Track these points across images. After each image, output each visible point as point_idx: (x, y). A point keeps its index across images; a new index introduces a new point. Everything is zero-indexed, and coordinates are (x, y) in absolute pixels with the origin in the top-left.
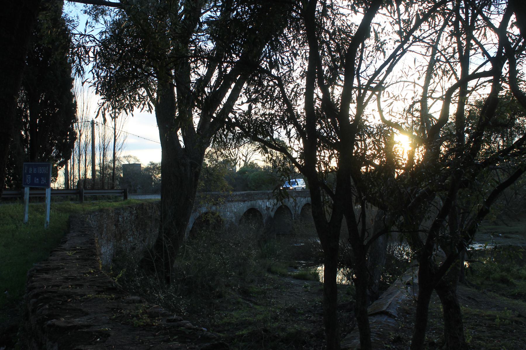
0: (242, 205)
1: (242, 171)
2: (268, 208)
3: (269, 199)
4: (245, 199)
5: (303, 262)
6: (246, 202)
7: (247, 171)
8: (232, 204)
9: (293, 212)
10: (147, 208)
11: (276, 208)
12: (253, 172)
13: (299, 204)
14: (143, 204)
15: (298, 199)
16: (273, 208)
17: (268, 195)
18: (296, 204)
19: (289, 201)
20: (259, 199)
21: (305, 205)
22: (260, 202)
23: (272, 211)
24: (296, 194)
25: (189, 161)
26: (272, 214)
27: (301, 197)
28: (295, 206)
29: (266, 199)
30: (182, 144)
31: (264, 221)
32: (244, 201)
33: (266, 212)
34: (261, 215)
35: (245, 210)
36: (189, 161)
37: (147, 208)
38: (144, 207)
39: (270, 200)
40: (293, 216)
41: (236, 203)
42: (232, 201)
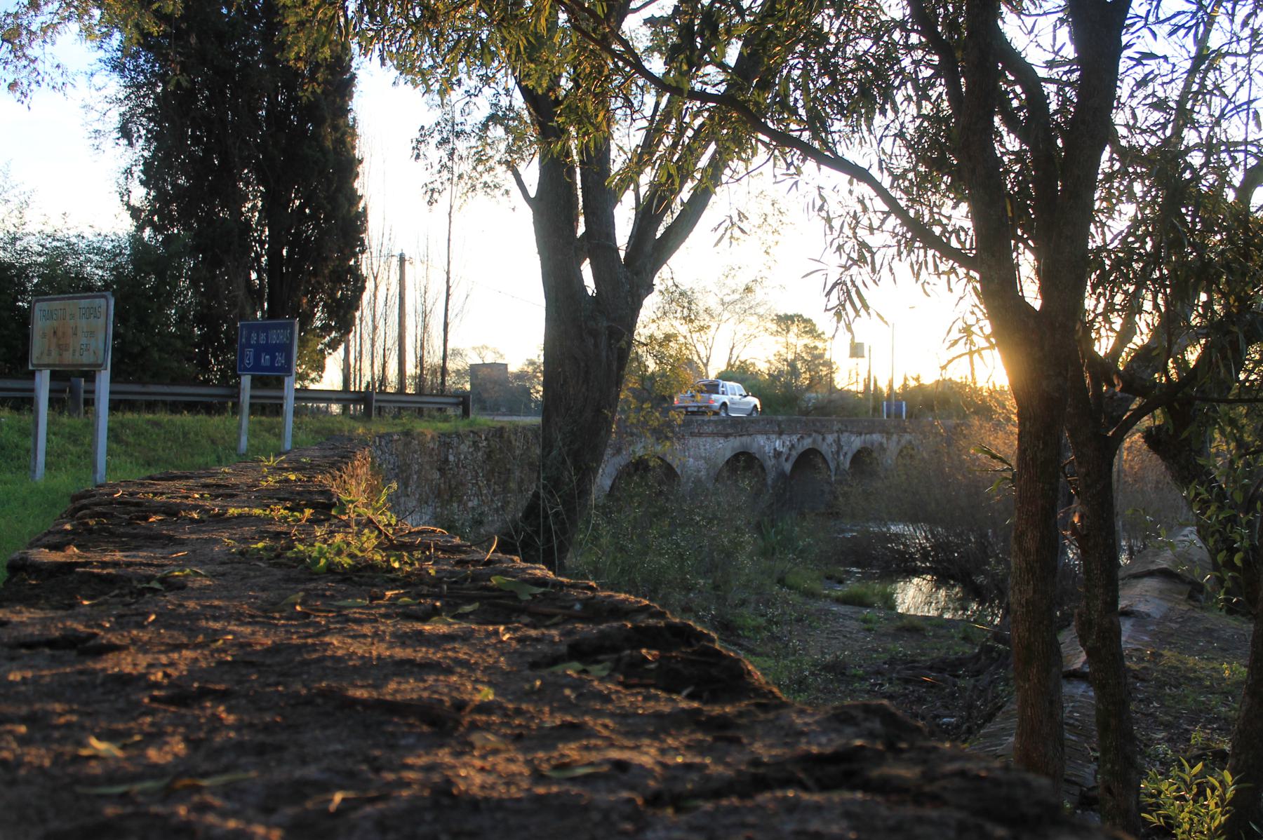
2: (778, 454)
3: (781, 433)
4: (729, 431)
5: (855, 569)
6: (731, 439)
8: (701, 441)
9: (832, 466)
11: (795, 454)
13: (845, 449)
16: (789, 455)
17: (779, 426)
18: (840, 447)
19: (824, 439)
22: (761, 440)
23: (787, 460)
24: (840, 425)
26: (788, 467)
27: (852, 432)
28: (838, 453)
29: (774, 432)
31: (769, 482)
32: (727, 436)
33: (773, 461)
34: (763, 469)
35: (729, 454)
37: (513, 437)
38: (506, 435)
39: (784, 437)
41: (709, 440)
42: (700, 435)
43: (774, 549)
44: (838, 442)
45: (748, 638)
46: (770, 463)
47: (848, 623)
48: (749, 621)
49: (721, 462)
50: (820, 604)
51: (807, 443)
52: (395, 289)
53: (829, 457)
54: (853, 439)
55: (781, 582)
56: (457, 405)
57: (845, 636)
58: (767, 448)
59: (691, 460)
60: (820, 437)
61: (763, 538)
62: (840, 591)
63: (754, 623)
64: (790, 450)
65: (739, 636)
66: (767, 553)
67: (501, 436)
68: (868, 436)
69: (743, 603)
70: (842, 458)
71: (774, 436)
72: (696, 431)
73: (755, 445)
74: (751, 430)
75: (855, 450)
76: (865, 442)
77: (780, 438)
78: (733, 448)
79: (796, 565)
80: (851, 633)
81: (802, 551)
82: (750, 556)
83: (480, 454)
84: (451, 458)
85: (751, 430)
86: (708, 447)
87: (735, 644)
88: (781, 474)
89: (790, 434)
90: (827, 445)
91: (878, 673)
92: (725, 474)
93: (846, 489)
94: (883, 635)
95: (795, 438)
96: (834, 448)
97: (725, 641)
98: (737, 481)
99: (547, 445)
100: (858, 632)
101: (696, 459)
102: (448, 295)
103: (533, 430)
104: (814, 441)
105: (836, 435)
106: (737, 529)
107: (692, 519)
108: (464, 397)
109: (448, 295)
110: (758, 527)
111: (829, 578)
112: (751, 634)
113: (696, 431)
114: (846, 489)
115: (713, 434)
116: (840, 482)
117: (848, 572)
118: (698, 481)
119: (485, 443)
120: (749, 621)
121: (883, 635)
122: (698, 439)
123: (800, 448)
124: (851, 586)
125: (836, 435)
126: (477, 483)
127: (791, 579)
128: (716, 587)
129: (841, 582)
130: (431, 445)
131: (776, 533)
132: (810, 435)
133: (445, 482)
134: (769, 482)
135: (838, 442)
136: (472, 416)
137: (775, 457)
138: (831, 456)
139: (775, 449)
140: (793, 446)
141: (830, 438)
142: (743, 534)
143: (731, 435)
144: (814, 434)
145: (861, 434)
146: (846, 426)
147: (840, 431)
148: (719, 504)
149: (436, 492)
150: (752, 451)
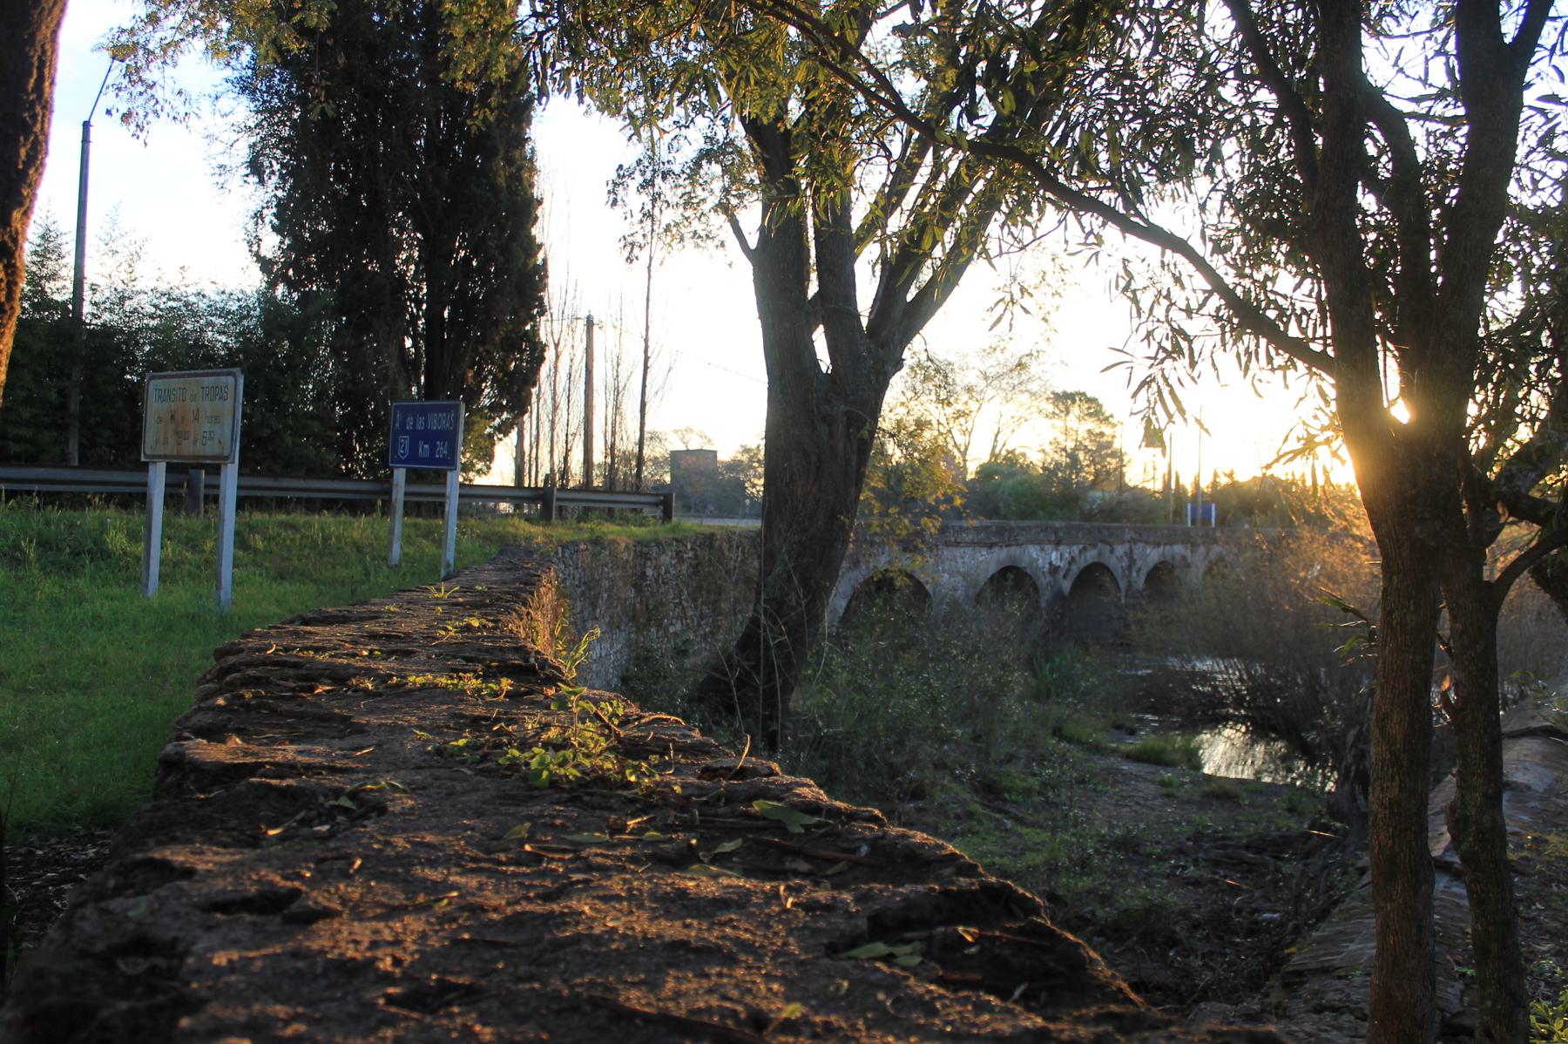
0: (983, 555)
2: (1054, 570)
3: (1058, 543)
4: (994, 539)
5: (1149, 717)
6: (996, 549)
8: (958, 552)
9: (1123, 585)
10: (725, 546)
11: (1075, 569)
13: (1139, 563)
16: (1068, 570)
18: (1132, 561)
19: (1112, 551)
22: (1033, 551)
23: (1065, 576)
24: (1132, 534)
26: (1066, 585)
27: (1147, 542)
28: (1130, 568)
29: (1050, 542)
31: (1043, 604)
32: (990, 546)
33: (1049, 578)
34: (1036, 588)
35: (993, 569)
37: (725, 546)
38: (717, 544)
39: (1061, 548)
41: (969, 550)
42: (957, 544)
43: (1049, 690)
44: (1130, 554)
46: (1044, 581)
47: (1141, 786)
48: (1018, 781)
49: (983, 579)
51: (1091, 556)
53: (1118, 573)
54: (1148, 551)
55: (1058, 732)
56: (656, 505)
57: (1137, 803)
58: (1040, 561)
59: (946, 575)
60: (1108, 548)
61: (1035, 676)
62: (1132, 744)
63: (1024, 784)
64: (1070, 563)
65: (1005, 800)
66: (1040, 695)
67: (711, 546)
68: (1168, 548)
69: (1010, 758)
70: (1134, 574)
73: (1026, 558)
74: (1021, 539)
75: (1151, 565)
76: (1163, 554)
77: (1057, 550)
79: (1077, 711)
80: (1146, 799)
81: (1084, 694)
82: (1020, 700)
83: (684, 567)
84: (649, 572)
85: (1021, 539)
86: (966, 560)
87: (1000, 811)
89: (1070, 544)
90: (1116, 557)
91: (1180, 852)
92: (988, 594)
95: (1076, 549)
96: (1125, 563)
97: (988, 807)
98: (1003, 604)
99: (769, 558)
100: (1155, 798)
101: (951, 575)
102: (646, 368)
103: (752, 538)
104: (1100, 554)
105: (1127, 546)
106: (1004, 666)
108: (665, 496)
109: (646, 368)
110: (1030, 663)
111: (1118, 727)
112: (1020, 798)
114: (1140, 615)
115: (972, 544)
117: (1141, 720)
118: (954, 604)
119: (691, 554)
122: (954, 549)
124: (1144, 739)
125: (1127, 546)
126: (680, 603)
127: (1070, 729)
128: (976, 738)
129: (1132, 732)
131: (1052, 671)
132: (1095, 546)
135: (1130, 554)
136: (675, 519)
137: (1050, 573)
139: (1051, 563)
140: (1073, 559)
141: (1120, 550)
142: (1012, 672)
144: (1100, 545)
147: (1133, 541)
148: (980, 633)
150: (1022, 565)
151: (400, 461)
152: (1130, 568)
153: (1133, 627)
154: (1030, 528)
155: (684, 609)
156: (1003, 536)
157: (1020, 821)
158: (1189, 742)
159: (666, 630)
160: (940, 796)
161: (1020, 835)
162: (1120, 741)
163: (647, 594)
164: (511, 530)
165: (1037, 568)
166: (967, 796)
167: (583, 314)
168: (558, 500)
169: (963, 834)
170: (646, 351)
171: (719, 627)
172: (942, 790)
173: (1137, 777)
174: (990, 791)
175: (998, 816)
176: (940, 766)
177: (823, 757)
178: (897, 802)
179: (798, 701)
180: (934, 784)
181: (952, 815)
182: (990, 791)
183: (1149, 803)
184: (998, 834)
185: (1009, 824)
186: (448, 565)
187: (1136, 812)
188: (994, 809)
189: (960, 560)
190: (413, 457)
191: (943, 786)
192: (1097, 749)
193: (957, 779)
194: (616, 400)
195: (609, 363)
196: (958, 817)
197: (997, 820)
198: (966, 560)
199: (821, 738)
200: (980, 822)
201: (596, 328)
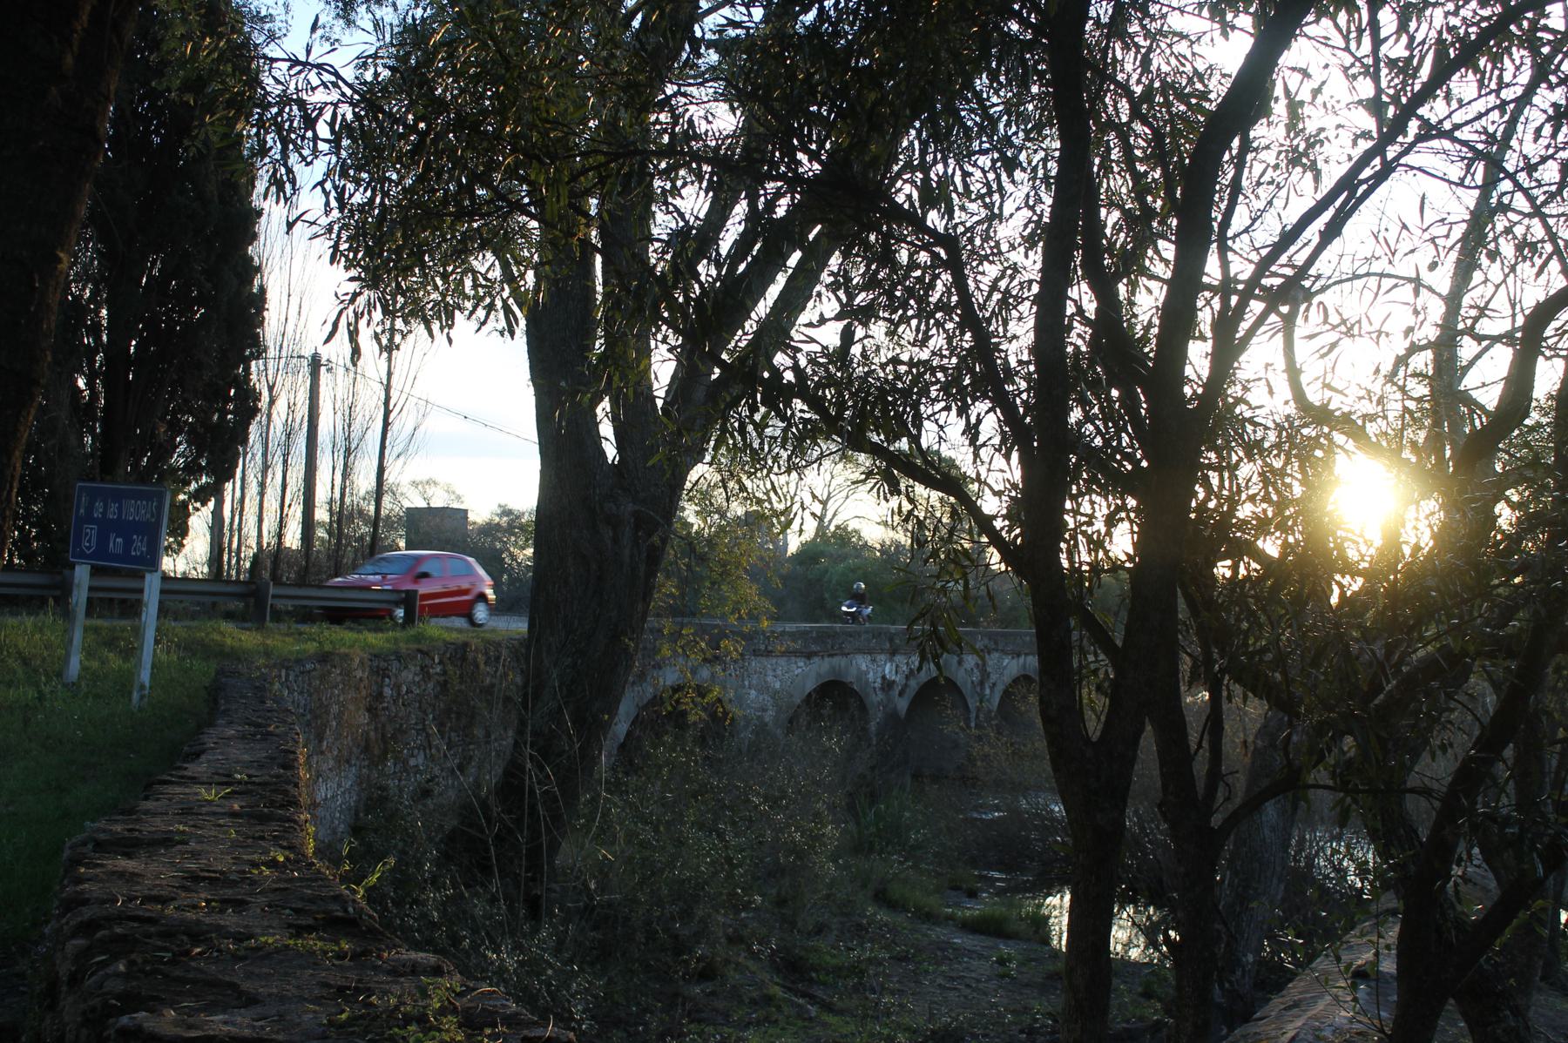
0: (799, 667)
1: (809, 554)
2: (888, 685)
3: (893, 653)
4: (814, 648)
5: (997, 875)
6: (816, 659)
7: (822, 554)
8: (768, 663)
9: (973, 703)
10: (481, 658)
11: (913, 683)
12: (844, 558)
13: (994, 677)
14: (466, 645)
15: (992, 660)
16: (906, 685)
17: (891, 640)
18: (985, 675)
19: (960, 663)
20: (860, 651)
21: (1016, 681)
22: (862, 662)
23: (901, 694)
24: (986, 641)
25: (630, 507)
26: (902, 705)
27: (1004, 652)
28: (982, 683)
29: (882, 651)
30: (611, 451)
31: (873, 726)
32: (809, 656)
33: (880, 696)
34: (863, 707)
35: (810, 685)
36: (630, 507)
37: (481, 658)
38: (470, 656)
39: (898, 658)
40: (973, 715)
41: (782, 661)
42: (768, 653)
45: (824, 984)
48: (828, 958)
49: (798, 701)
50: (938, 933)
52: (302, 410)
53: (967, 690)
55: (882, 898)
57: (968, 986)
58: (871, 675)
59: (753, 692)
60: (956, 659)
62: (973, 910)
63: (834, 961)
64: (907, 678)
65: (811, 980)
66: (859, 847)
67: (464, 659)
69: (820, 930)
70: (988, 691)
71: (883, 657)
72: (763, 647)
73: (853, 671)
75: (1007, 679)
76: (1024, 666)
77: (891, 660)
78: (819, 675)
80: (978, 981)
83: (430, 685)
84: (387, 691)
86: (779, 672)
87: (804, 995)
88: (892, 716)
90: (964, 669)
93: (987, 749)
94: (1027, 985)
96: (976, 677)
97: (790, 989)
100: (989, 979)
101: (760, 691)
107: (748, 801)
112: (830, 979)
113: (763, 647)
114: (987, 749)
115: (788, 653)
116: (979, 738)
118: (761, 729)
119: (438, 670)
120: (828, 958)
121: (1027, 985)
122: (763, 660)
123: (923, 677)
126: (424, 730)
128: (781, 902)
129: (972, 894)
130: (359, 674)
133: (376, 729)
134: (873, 726)
137: (882, 689)
138: (969, 685)
139: (884, 677)
140: (911, 671)
141: (970, 660)
143: (815, 654)
145: (1019, 655)
146: (996, 643)
149: (363, 744)
150: (850, 679)
151: (82, 555)
152: (982, 683)
153: (979, 763)
154: (859, 634)
155: (428, 736)
156: (826, 644)
157: (828, 1008)
158: (1040, 906)
159: (405, 762)
160: (734, 977)
161: (825, 1025)
162: (957, 905)
163: (383, 719)
164: (217, 637)
165: (867, 681)
166: (766, 976)
167: (308, 353)
168: (274, 596)
169: (758, 1023)
170: (387, 403)
171: (471, 758)
172: (735, 970)
173: (970, 953)
174: (793, 969)
175: (801, 1001)
176: (735, 940)
177: (595, 928)
178: (681, 983)
179: (568, 854)
180: (727, 962)
181: (747, 1001)
182: (793, 969)
183: (981, 986)
184: (800, 1023)
185: (813, 1010)
186: (142, 687)
187: (965, 997)
188: (797, 993)
189: (770, 673)
190: (102, 552)
191: (738, 964)
192: (929, 917)
193: (754, 956)
194: (346, 465)
195: (339, 414)
196: (754, 1002)
197: (799, 1006)
198: (779, 672)
199: (594, 908)
200: (779, 1008)
201: (323, 369)
